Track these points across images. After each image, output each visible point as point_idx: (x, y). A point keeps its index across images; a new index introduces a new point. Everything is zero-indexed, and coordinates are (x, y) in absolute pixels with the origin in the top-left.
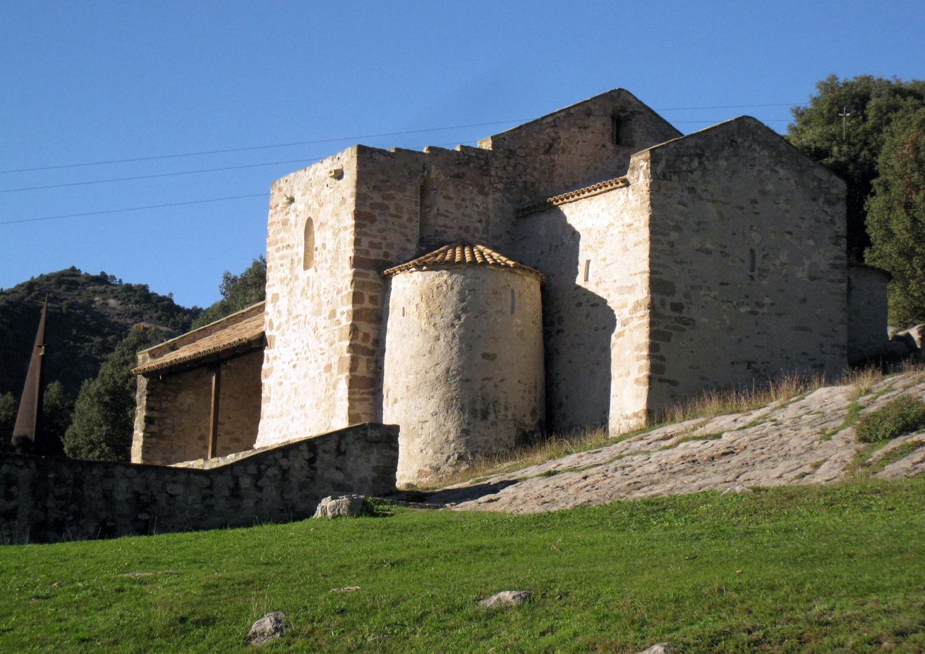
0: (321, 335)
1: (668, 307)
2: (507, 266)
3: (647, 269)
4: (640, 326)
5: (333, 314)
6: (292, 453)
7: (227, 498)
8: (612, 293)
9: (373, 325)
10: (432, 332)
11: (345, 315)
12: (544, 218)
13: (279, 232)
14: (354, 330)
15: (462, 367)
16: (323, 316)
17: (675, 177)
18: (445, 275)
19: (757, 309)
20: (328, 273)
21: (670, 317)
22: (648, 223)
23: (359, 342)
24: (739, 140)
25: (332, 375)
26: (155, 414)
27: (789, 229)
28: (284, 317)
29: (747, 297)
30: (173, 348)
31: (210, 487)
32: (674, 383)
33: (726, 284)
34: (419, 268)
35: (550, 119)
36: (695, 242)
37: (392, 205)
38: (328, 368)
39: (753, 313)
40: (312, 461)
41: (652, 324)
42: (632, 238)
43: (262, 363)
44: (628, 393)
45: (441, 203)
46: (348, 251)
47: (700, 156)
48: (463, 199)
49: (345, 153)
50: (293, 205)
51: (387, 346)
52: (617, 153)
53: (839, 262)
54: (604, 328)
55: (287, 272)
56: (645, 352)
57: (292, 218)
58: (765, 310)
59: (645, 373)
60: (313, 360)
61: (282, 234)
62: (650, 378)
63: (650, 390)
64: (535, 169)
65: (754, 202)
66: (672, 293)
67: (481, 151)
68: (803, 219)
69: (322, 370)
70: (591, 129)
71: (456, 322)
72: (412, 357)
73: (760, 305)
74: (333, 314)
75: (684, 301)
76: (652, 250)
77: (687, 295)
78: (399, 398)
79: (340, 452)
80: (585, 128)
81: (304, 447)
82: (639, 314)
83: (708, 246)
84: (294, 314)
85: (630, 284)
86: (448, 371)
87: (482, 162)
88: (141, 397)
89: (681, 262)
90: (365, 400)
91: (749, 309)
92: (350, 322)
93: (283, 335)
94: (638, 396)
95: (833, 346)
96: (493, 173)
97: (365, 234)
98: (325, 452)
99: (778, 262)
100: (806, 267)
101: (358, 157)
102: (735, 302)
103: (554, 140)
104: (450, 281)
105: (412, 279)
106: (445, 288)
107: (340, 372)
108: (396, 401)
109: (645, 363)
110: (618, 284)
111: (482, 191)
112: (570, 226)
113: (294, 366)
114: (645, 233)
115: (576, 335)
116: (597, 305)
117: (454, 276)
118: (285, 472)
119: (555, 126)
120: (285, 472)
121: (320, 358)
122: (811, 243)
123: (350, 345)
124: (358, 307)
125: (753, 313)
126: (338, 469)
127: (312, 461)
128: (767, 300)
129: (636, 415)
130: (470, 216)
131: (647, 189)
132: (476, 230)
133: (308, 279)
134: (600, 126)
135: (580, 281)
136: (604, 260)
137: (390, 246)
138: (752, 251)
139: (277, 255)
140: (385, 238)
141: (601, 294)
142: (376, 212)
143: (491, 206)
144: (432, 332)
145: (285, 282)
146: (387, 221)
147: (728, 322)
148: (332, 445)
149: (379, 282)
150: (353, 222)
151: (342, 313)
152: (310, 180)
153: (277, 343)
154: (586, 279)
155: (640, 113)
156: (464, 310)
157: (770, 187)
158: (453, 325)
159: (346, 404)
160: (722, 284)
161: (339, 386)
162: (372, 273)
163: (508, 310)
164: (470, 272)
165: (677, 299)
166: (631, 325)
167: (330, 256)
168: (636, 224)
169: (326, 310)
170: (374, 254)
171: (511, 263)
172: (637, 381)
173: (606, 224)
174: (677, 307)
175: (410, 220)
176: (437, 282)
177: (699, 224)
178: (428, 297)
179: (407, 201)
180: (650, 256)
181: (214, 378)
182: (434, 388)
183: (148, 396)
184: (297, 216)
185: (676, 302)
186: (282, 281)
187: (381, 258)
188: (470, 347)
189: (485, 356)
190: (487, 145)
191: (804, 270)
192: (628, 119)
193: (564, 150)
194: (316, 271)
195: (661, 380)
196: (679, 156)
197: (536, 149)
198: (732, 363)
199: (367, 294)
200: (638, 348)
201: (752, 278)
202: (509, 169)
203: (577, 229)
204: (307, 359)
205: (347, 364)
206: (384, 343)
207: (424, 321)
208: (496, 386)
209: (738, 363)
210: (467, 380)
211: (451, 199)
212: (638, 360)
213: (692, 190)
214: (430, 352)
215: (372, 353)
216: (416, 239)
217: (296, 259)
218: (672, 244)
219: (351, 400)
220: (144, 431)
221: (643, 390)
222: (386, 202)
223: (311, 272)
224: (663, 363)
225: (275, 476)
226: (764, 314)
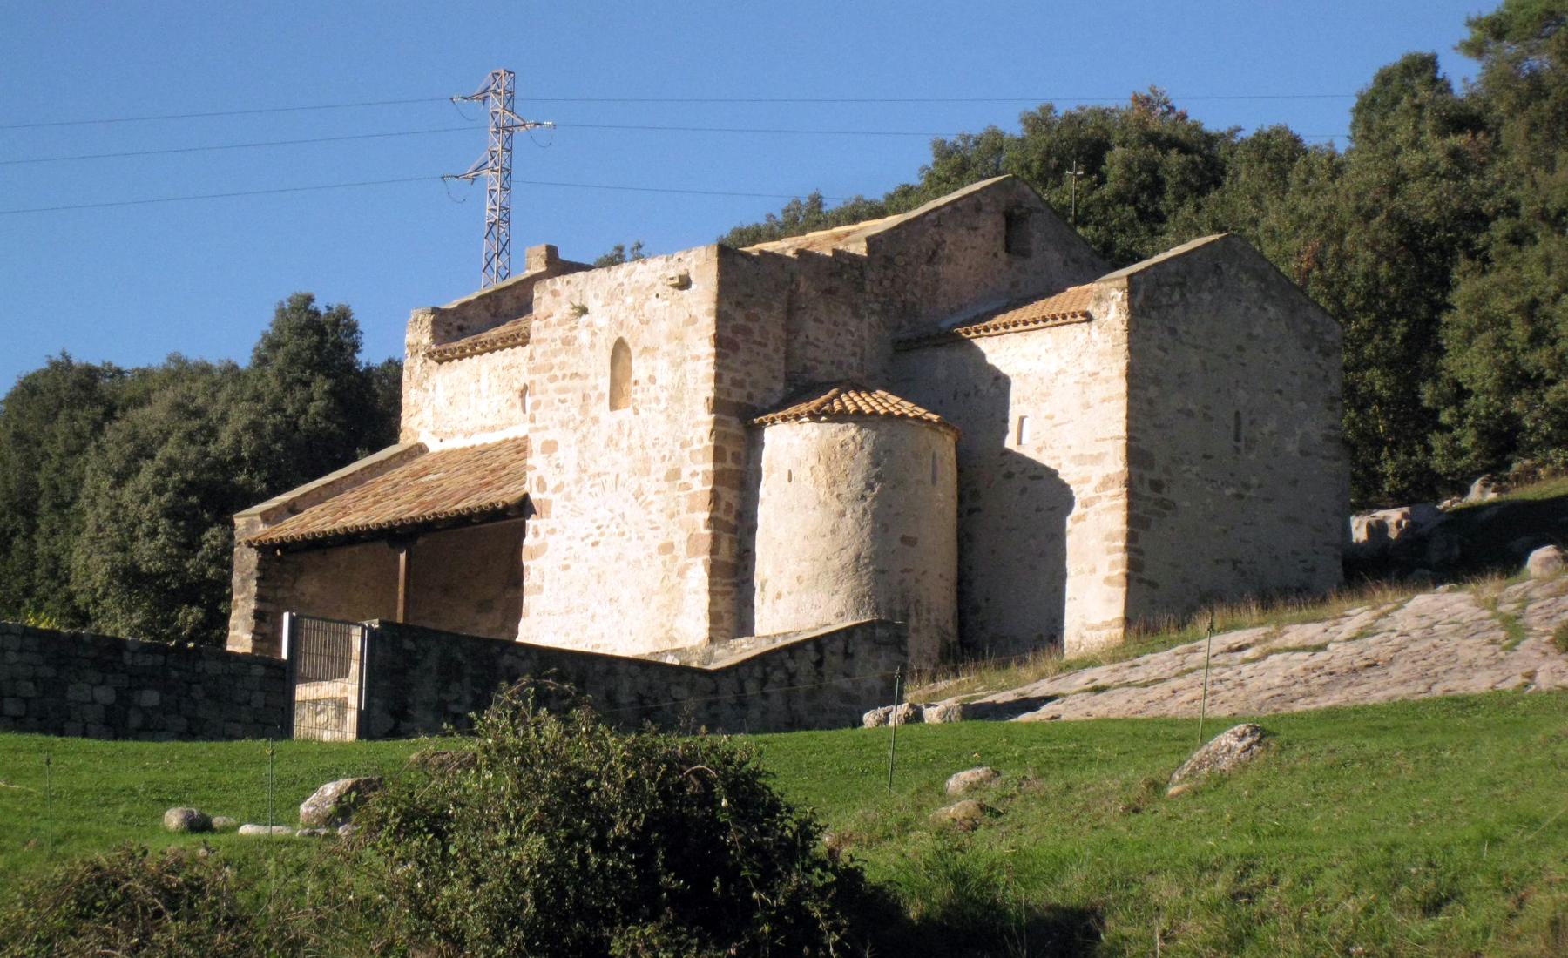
0: (651, 503)
1: (1146, 485)
2: (929, 421)
3: (1123, 433)
4: (1113, 508)
5: (674, 475)
6: (799, 653)
7: (732, 706)
8: (1065, 463)
9: (735, 492)
10: (836, 505)
11: (700, 477)
12: (942, 353)
13: (555, 354)
14: (715, 497)
15: (876, 553)
16: (653, 477)
17: (1154, 313)
18: (852, 429)
19: (1243, 492)
20: (662, 418)
21: (1149, 499)
22: (1124, 372)
23: (720, 515)
24: (1224, 266)
25: (675, 559)
26: (269, 607)
27: (1280, 387)
28: (570, 474)
30: (292, 509)
31: (715, 692)
32: (1153, 584)
34: (814, 417)
35: (933, 216)
37: (755, 327)
38: (667, 548)
39: (1239, 496)
40: (819, 663)
41: (1130, 506)
42: (1098, 391)
43: (522, 535)
44: (1093, 598)
45: (811, 329)
46: (707, 390)
47: (1182, 285)
48: (835, 324)
49: (692, 254)
50: (585, 318)
51: (760, 520)
52: (1009, 264)
54: (1052, 509)
55: (575, 411)
56: (1121, 543)
57: (584, 337)
58: (1252, 493)
59: (1120, 570)
60: (634, 537)
61: (562, 357)
62: (1128, 576)
63: (1128, 594)
64: (916, 283)
65: (1240, 348)
66: (1152, 467)
67: (854, 258)
68: (1294, 373)
69: (654, 550)
71: (868, 493)
72: (806, 537)
73: (1247, 487)
74: (674, 475)
75: (1164, 477)
76: (1130, 408)
77: (1166, 470)
78: (784, 592)
79: (848, 655)
80: (976, 229)
81: (810, 647)
82: (1110, 493)
83: (1191, 406)
84: (592, 469)
85: (1095, 453)
86: (858, 557)
87: (857, 273)
88: (244, 581)
89: (1160, 427)
90: (729, 593)
92: (710, 487)
93: (568, 498)
94: (1110, 601)
95: (1326, 544)
96: (868, 288)
97: (727, 367)
98: (832, 653)
99: (1266, 430)
101: (719, 262)
103: (938, 245)
104: (858, 438)
105: (803, 433)
106: (852, 446)
107: (693, 551)
108: (779, 596)
109: (1120, 557)
110: (1076, 451)
111: (856, 314)
112: (991, 367)
113: (595, 544)
114: (1122, 386)
115: (1003, 517)
116: (1040, 478)
117: (864, 432)
118: (791, 676)
119: (939, 225)
120: (791, 676)
121: (649, 535)
122: (1303, 405)
123: (711, 519)
124: (720, 466)
126: (847, 675)
127: (819, 663)
128: (1254, 481)
129: (1107, 624)
130: (842, 347)
131: (1124, 327)
132: (850, 366)
133: (620, 424)
134: (991, 224)
135: (1010, 443)
136: (1051, 417)
137: (754, 384)
138: (1237, 413)
139: (553, 386)
140: (749, 374)
141: (1045, 460)
142: (739, 338)
143: (866, 334)
144: (836, 505)
145: (571, 425)
146: (750, 350)
147: (1212, 508)
148: (840, 644)
149: (741, 433)
150: (713, 350)
151: (694, 474)
152: (621, 285)
153: (555, 511)
154: (1019, 443)
155: (1039, 211)
156: (878, 477)
157: (1258, 331)
158: (863, 497)
159: (705, 599)
161: (689, 573)
162: (734, 421)
163: (928, 479)
164: (885, 427)
165: (1156, 474)
166: (1098, 506)
167: (664, 395)
168: (1104, 374)
169: (660, 469)
170: (737, 396)
171: (935, 417)
172: (1108, 580)
173: (1053, 369)
174: (1157, 486)
175: (776, 350)
176: (841, 438)
177: (1179, 376)
178: (829, 457)
179: (772, 323)
180: (1128, 417)
181: (403, 556)
182: (838, 580)
183: (258, 579)
184: (594, 334)
186: (563, 424)
187: (744, 400)
188: (885, 528)
189: (904, 540)
190: (860, 249)
192: (1022, 219)
193: (949, 260)
194: (636, 413)
195: (1140, 581)
196: (1159, 285)
197: (917, 257)
198: (1217, 561)
199: (730, 449)
200: (1110, 537)
201: (1238, 450)
202: (886, 283)
203: (1004, 370)
204: (623, 534)
205: (706, 543)
206: (754, 516)
207: (823, 490)
208: (917, 581)
210: (883, 572)
211: (821, 322)
212: (1109, 552)
213: (1173, 331)
214: (832, 532)
215: (734, 530)
216: (782, 376)
217: (594, 394)
218: (1151, 402)
219: (712, 593)
220: (254, 632)
221: (1119, 593)
222: (750, 325)
223: (624, 414)
225: (782, 681)
226: (1250, 498)
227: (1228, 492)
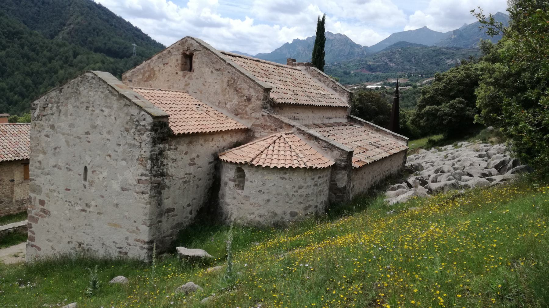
19: (86, 208)
29: (80, 199)
33: (69, 190)
36: (52, 162)
52: (184, 76)
58: (91, 209)
80: (167, 64)
91: (81, 208)
99: (101, 177)
100: (119, 181)
102: (73, 203)
122: (124, 163)
125: (83, 210)
128: (93, 203)
138: (86, 168)
147: (68, 215)
157: (99, 122)
174: (42, 202)
191: (118, 183)
201: (85, 187)
227: (78, 208)
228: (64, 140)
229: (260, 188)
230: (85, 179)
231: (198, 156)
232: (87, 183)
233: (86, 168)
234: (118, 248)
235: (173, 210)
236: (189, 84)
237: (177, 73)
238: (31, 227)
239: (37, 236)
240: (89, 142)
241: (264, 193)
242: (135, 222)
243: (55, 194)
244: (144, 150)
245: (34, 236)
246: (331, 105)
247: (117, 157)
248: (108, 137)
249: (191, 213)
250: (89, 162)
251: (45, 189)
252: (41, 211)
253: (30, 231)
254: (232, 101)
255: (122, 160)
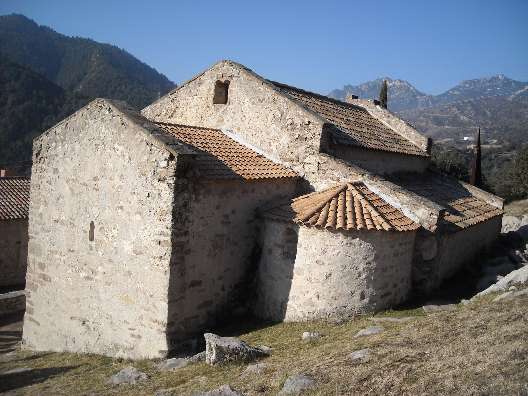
33: (73, 251)
39: (88, 278)
53: (162, 238)
58: (98, 277)
70: (200, 96)
91: (86, 275)
95: (151, 320)
99: (110, 235)
122: (138, 218)
125: (88, 278)
128: (100, 269)
138: (92, 224)
160: (70, 251)
174: (42, 266)
185: (42, 261)
198: (72, 318)
201: (91, 248)
209: (75, 318)
224: (32, 307)
226: (97, 280)
227: (83, 275)
228: (68, 187)
229: (318, 257)
230: (92, 239)
231: (233, 212)
232: (93, 243)
233: (92, 224)
234: (130, 329)
235: (199, 283)
236: (223, 120)
237: (208, 107)
238: (29, 297)
239: (35, 308)
240: (97, 190)
241: (323, 264)
242: (151, 296)
243: (57, 256)
244: (164, 200)
245: (32, 307)
246: (407, 152)
247: (130, 210)
248: (120, 183)
249: (223, 289)
250: (96, 216)
251: (46, 249)
252: (40, 277)
253: (29, 302)
254: (278, 141)
255: (137, 213)
